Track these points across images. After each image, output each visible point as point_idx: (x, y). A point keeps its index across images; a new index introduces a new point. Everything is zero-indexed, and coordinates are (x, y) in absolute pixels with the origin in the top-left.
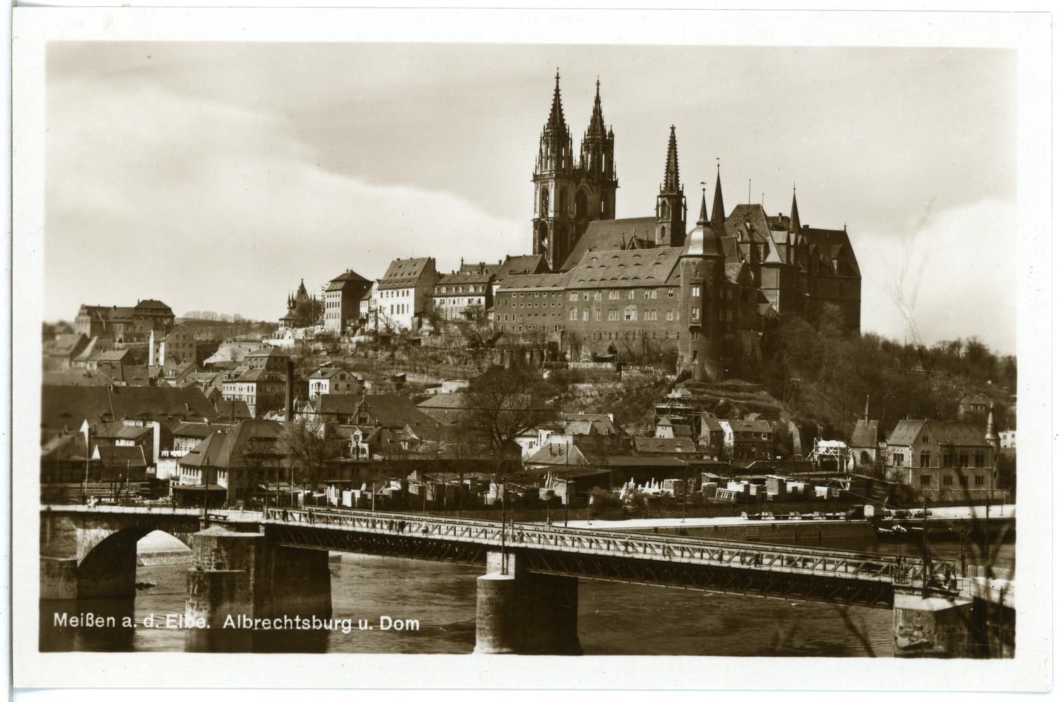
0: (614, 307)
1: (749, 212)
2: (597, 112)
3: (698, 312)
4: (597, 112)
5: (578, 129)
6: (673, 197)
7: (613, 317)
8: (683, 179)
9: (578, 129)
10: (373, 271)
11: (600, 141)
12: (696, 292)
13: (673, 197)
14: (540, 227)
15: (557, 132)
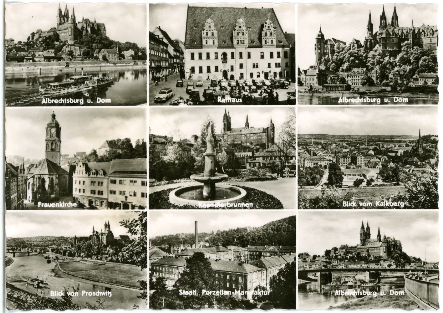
0: (373, 250)
1: (388, 238)
2: (368, 225)
3: (385, 250)
4: (368, 225)
5: (365, 227)
6: (379, 235)
7: (373, 251)
8: (381, 233)
9: (365, 227)
10: (338, 247)
11: (368, 228)
12: (385, 247)
13: (379, 235)
14: (361, 240)
15: (363, 227)
